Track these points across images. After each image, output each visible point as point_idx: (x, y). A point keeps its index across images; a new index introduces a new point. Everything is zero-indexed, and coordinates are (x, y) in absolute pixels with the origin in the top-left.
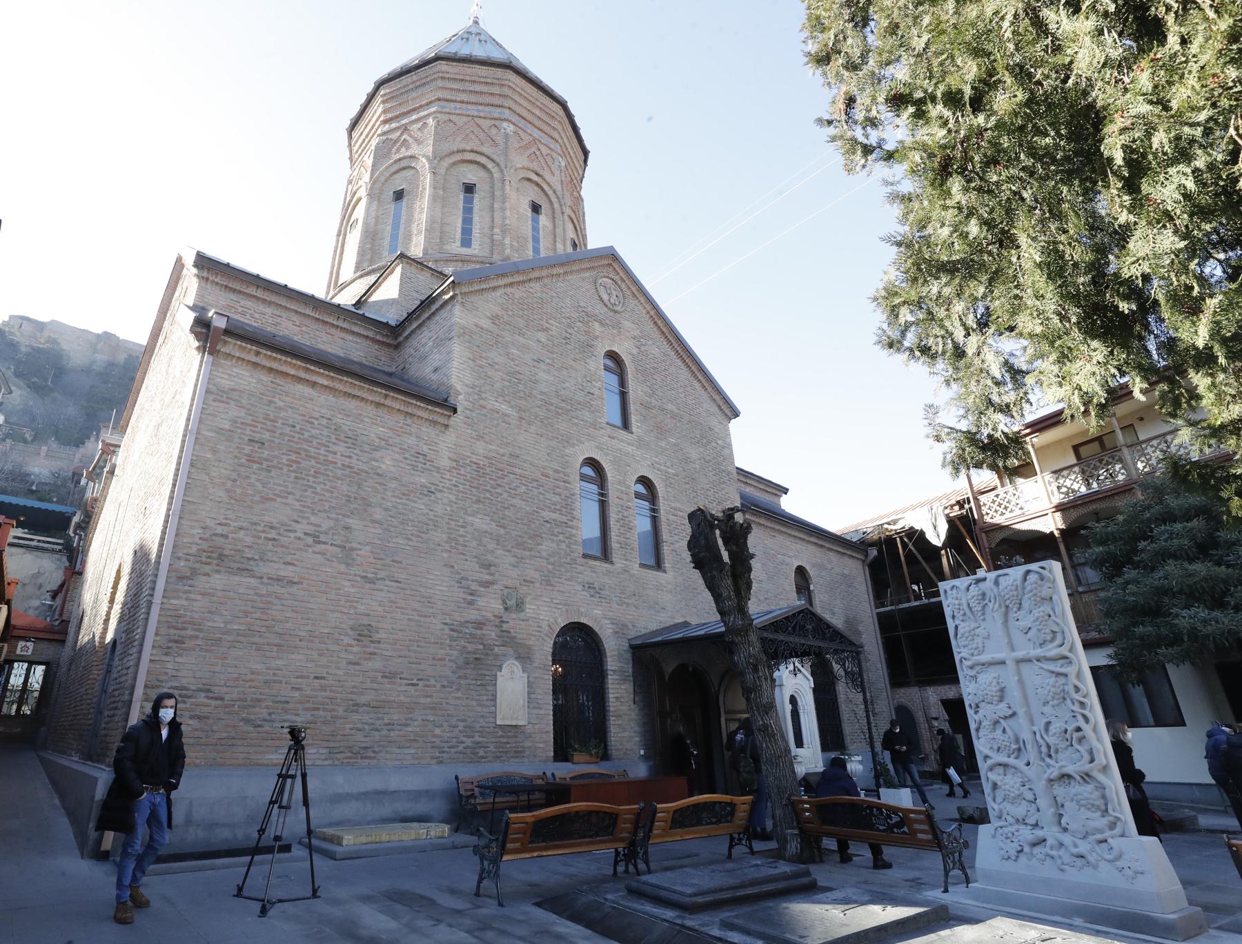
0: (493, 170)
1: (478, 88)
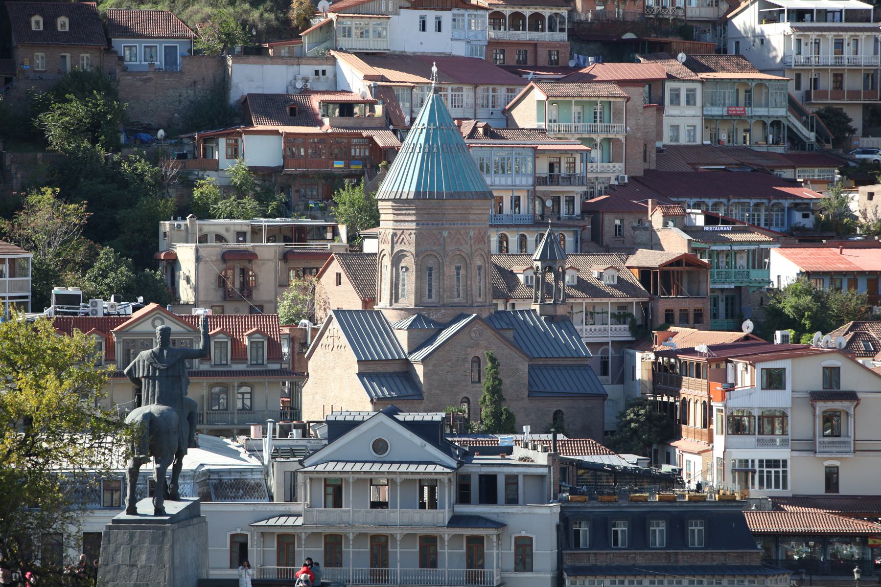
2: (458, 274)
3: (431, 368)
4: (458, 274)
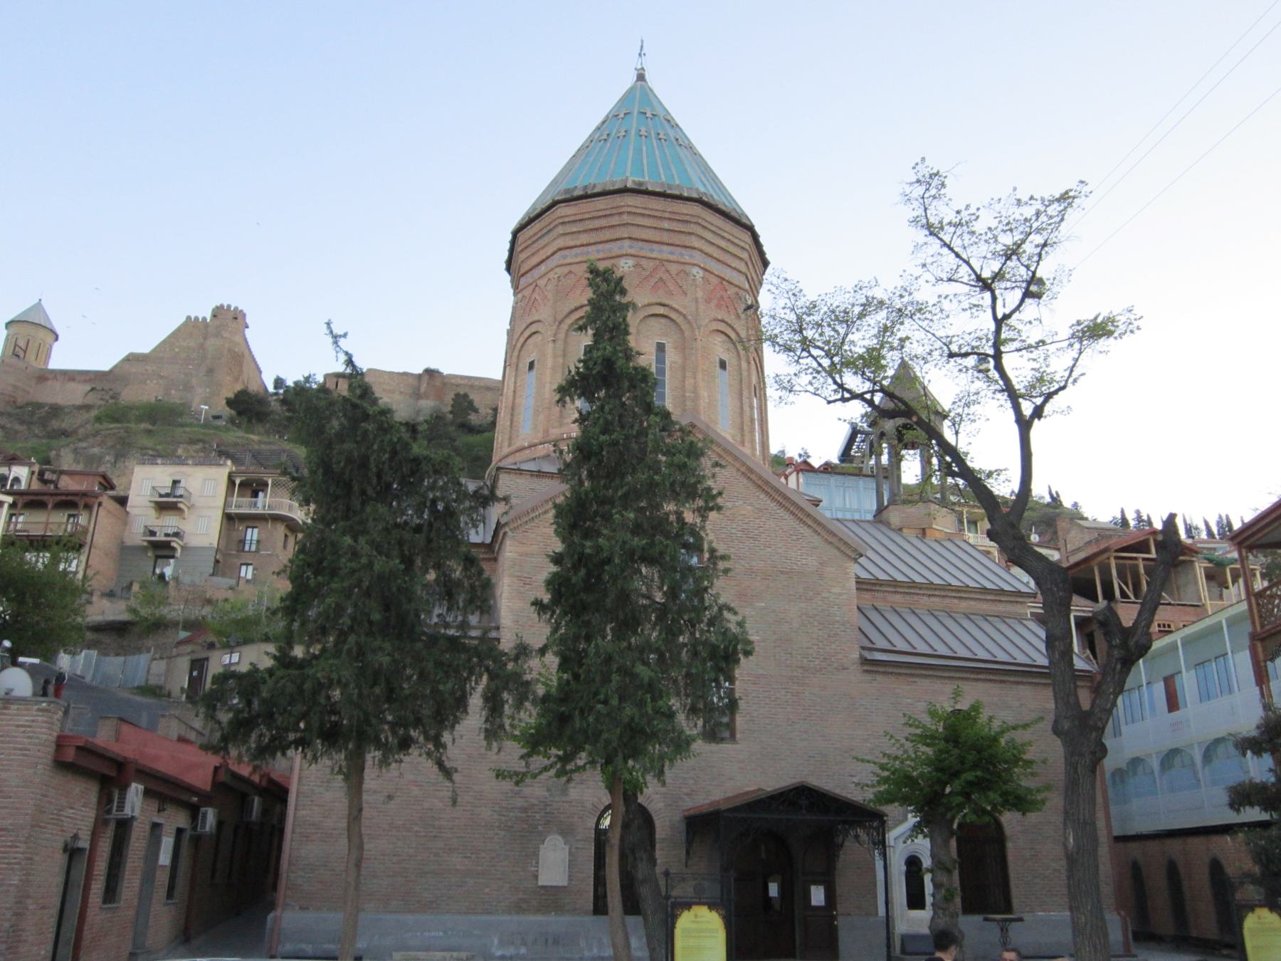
1: (597, 223)
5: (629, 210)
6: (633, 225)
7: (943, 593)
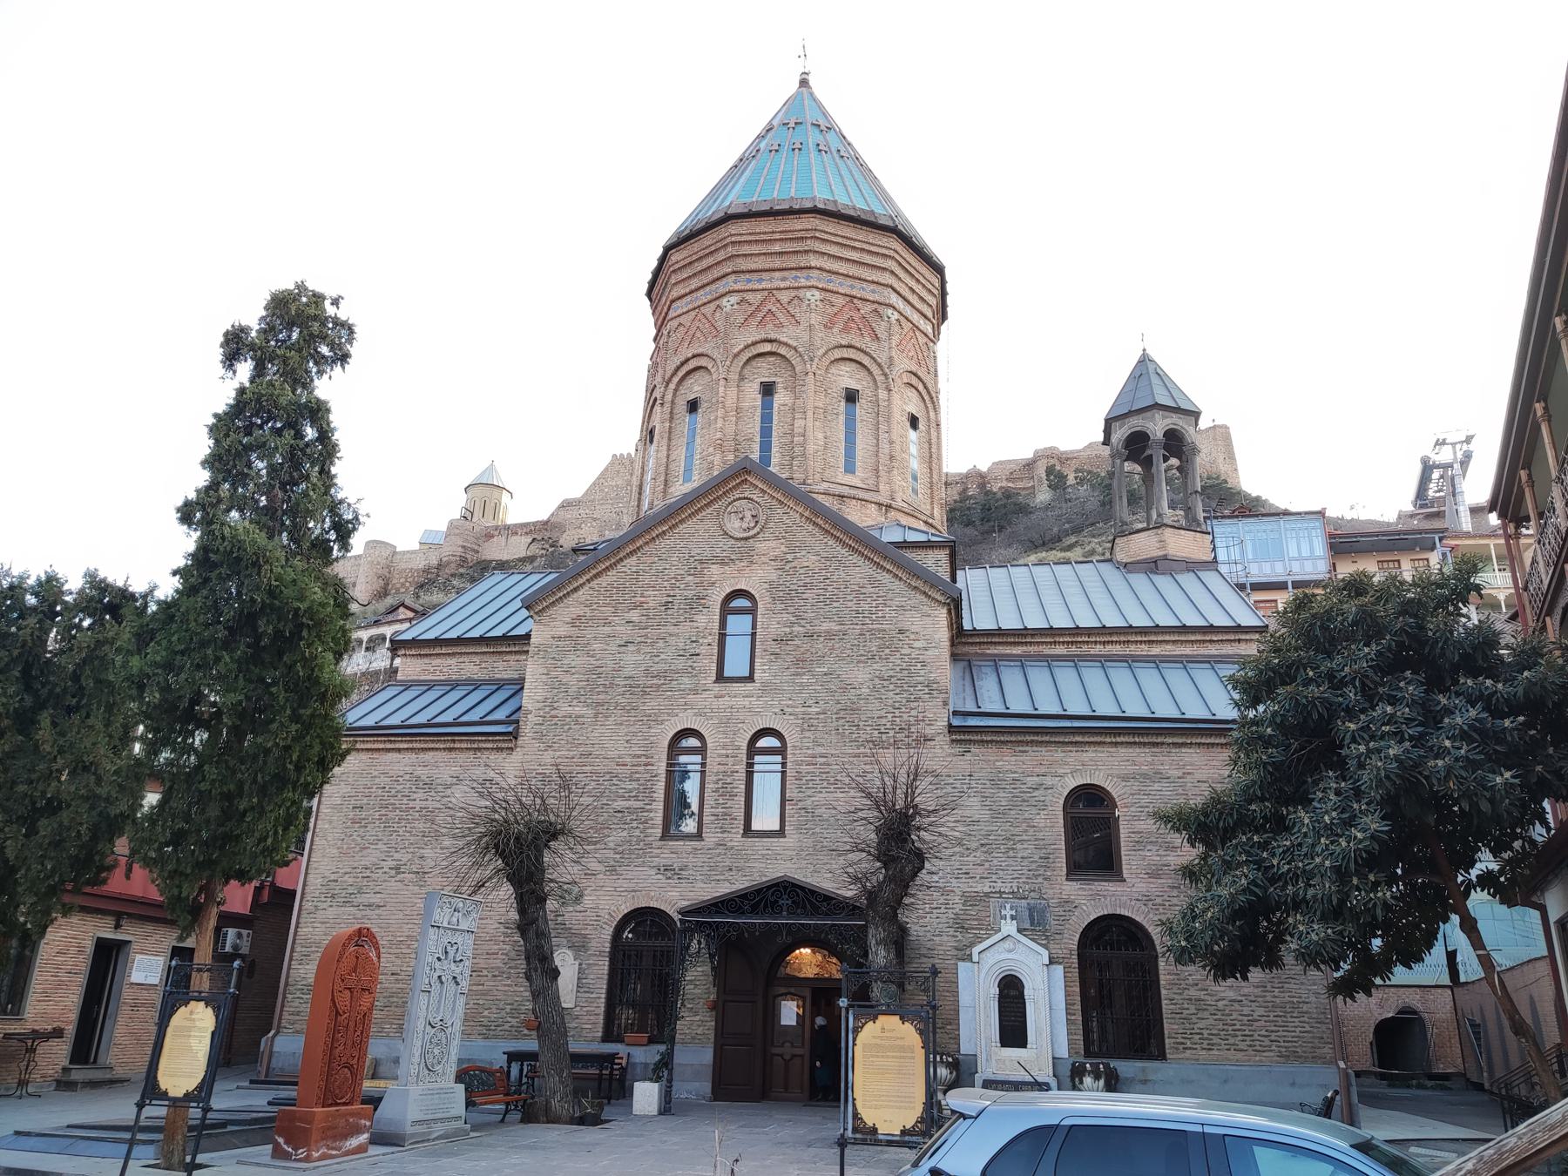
0: (712, 370)
2: (767, 407)
3: (563, 630)
4: (767, 407)
5: (733, 239)
6: (738, 256)
7: (1122, 638)
